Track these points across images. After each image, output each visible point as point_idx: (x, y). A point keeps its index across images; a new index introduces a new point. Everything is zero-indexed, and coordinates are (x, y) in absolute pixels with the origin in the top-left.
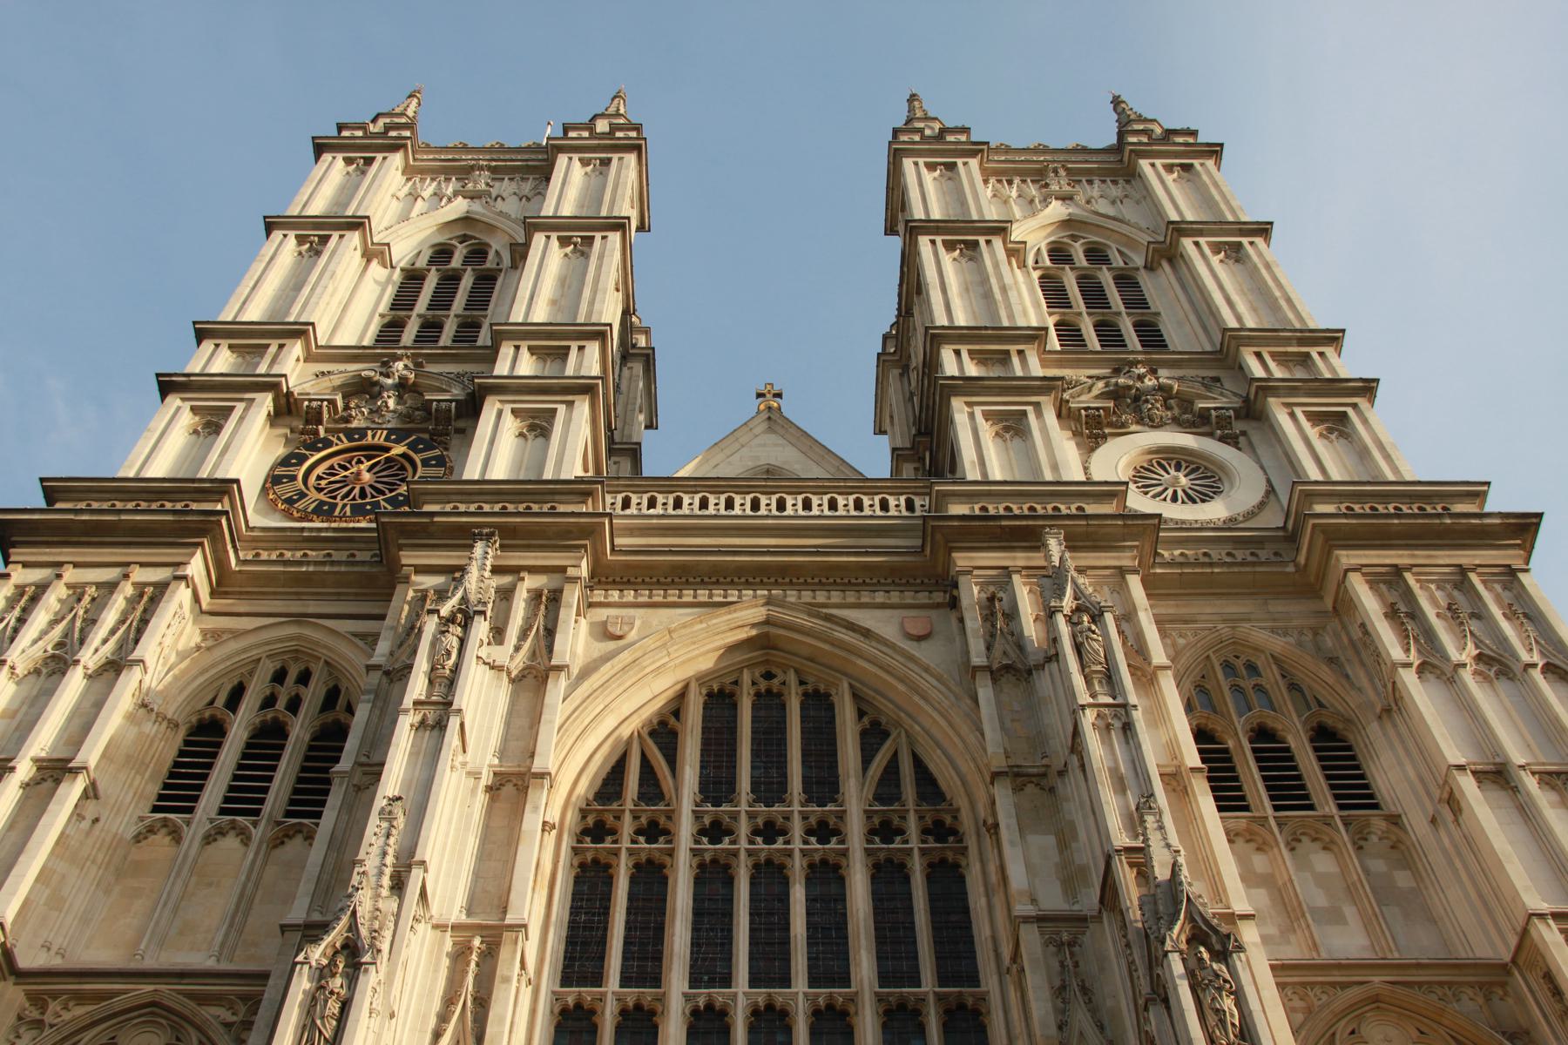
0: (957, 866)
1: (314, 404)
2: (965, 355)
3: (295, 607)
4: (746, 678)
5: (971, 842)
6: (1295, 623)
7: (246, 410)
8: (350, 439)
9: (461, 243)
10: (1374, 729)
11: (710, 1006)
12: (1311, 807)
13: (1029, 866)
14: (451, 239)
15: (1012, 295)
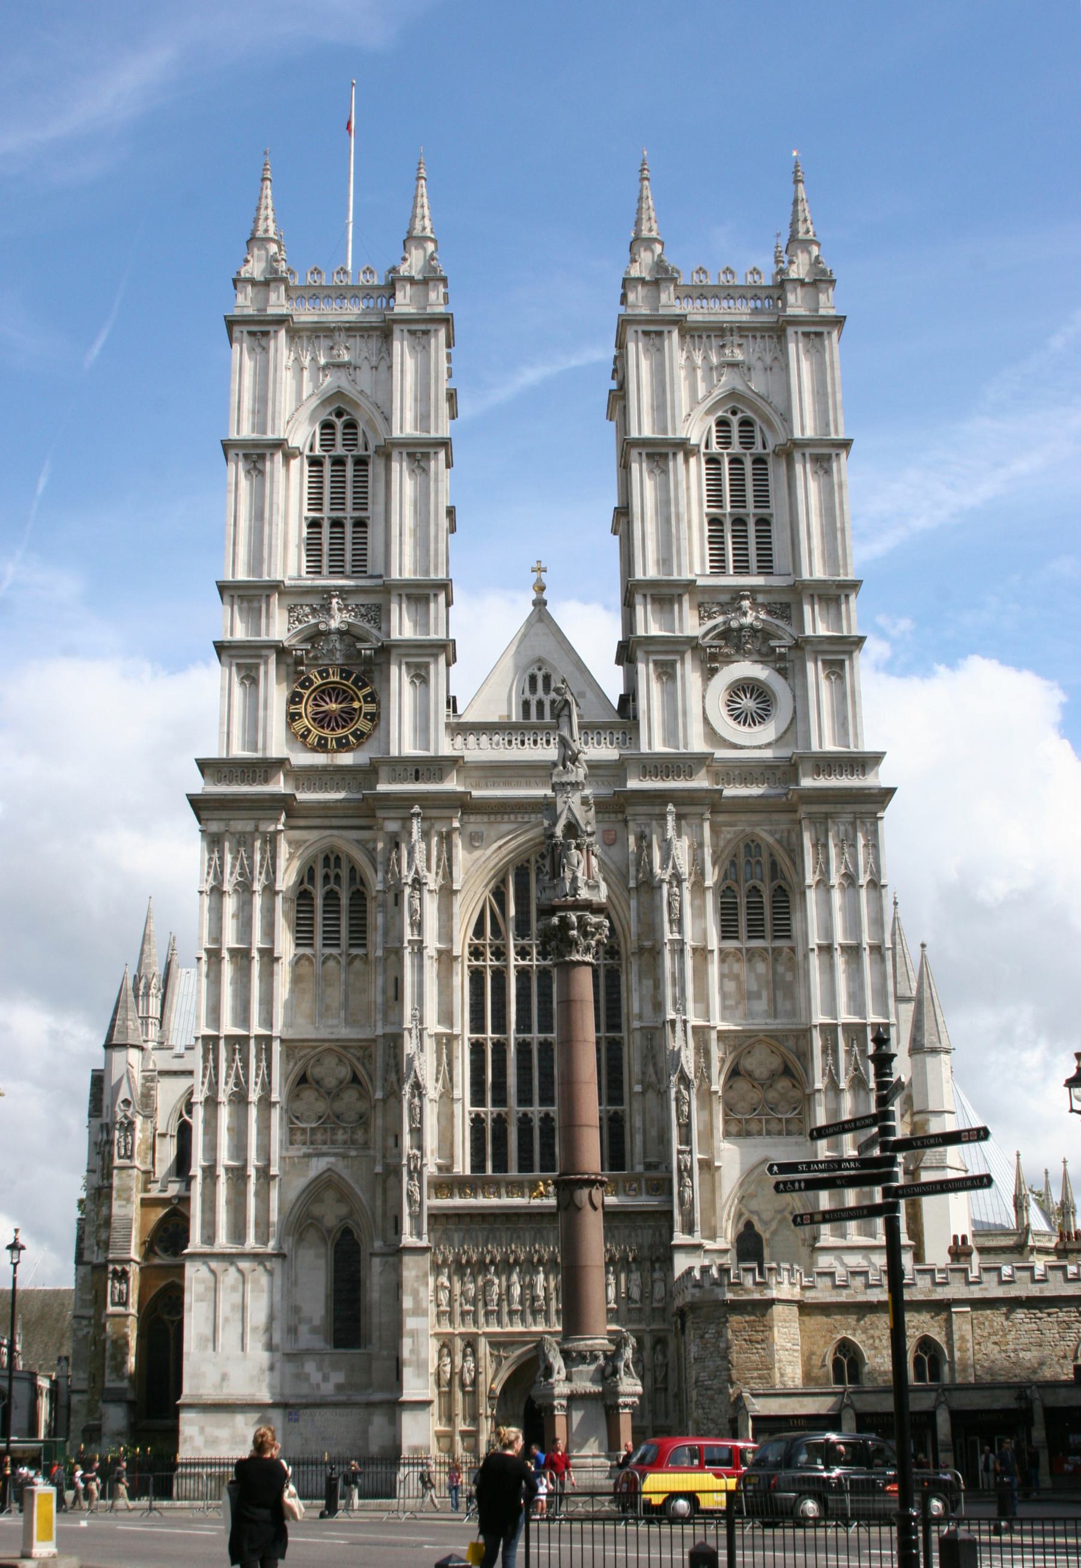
0: (618, 971)
1: (299, 653)
2: (649, 600)
3: (326, 822)
4: (533, 860)
5: (624, 963)
6: (782, 827)
7: (266, 663)
8: (323, 678)
9: (339, 414)
10: (798, 897)
11: (524, 1040)
12: (763, 937)
13: (641, 1000)
14: (330, 414)
15: (684, 526)
